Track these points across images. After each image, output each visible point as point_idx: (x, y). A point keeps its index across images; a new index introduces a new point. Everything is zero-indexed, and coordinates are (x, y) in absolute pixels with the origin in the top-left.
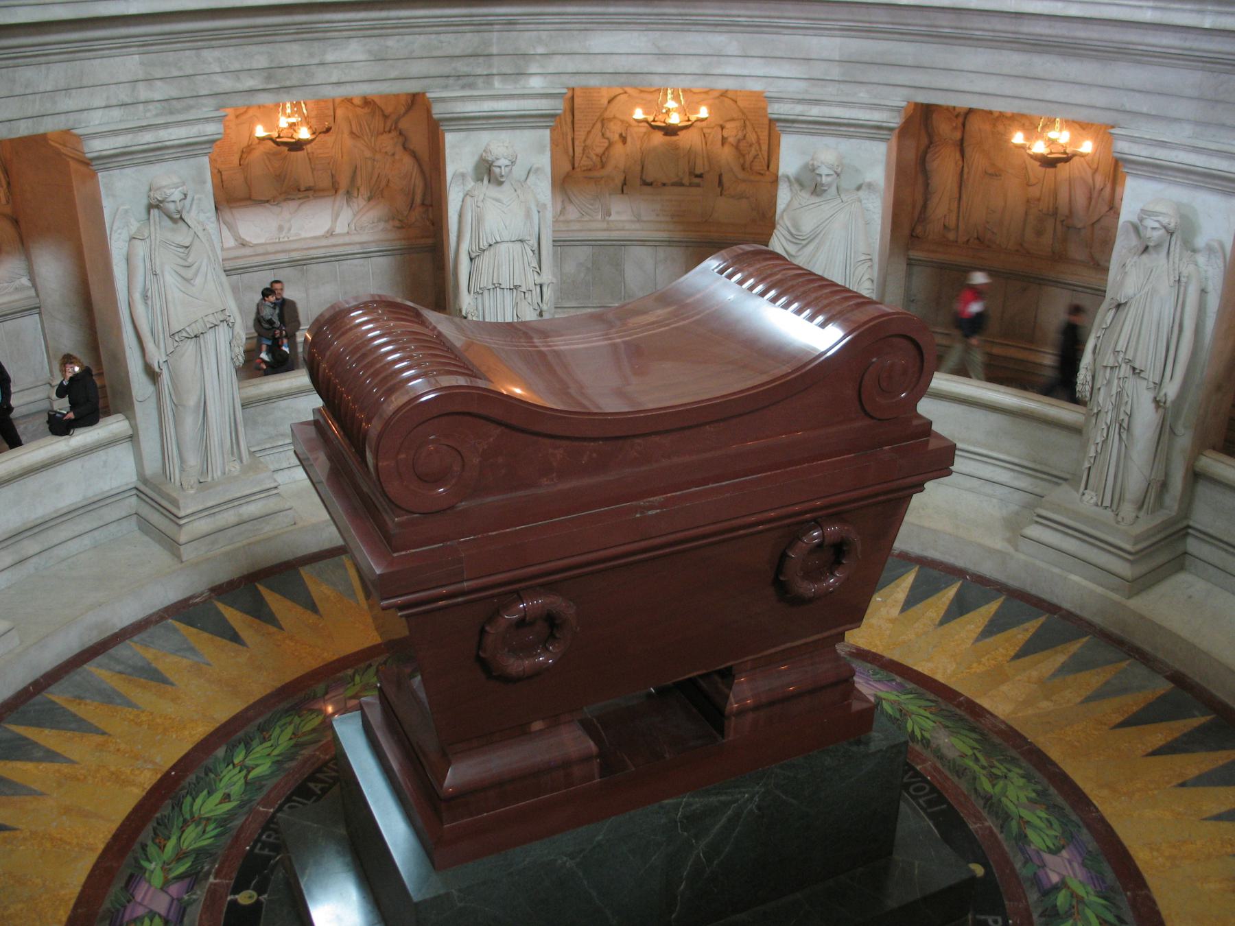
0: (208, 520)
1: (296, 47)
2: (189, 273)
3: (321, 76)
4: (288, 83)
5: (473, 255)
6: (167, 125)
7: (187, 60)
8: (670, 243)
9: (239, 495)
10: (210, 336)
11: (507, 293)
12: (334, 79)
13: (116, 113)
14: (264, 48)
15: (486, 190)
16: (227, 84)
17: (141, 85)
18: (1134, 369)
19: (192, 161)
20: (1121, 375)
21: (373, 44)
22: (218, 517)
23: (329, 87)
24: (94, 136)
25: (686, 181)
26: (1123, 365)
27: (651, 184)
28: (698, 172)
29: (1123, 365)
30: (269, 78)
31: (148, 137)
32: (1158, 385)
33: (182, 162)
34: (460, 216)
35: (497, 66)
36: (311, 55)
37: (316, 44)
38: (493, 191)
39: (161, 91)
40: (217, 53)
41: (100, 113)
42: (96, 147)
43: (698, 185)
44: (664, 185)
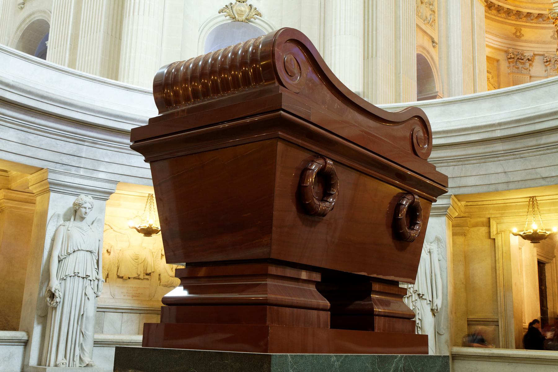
5: (62, 258)
8: (131, 311)
15: (72, 224)
18: (419, 294)
20: (414, 300)
25: (141, 277)
26: (413, 295)
27: (122, 278)
28: (148, 272)
29: (413, 295)
32: (432, 302)
34: (53, 240)
35: (83, 163)
38: (78, 223)
43: (148, 279)
44: (129, 278)
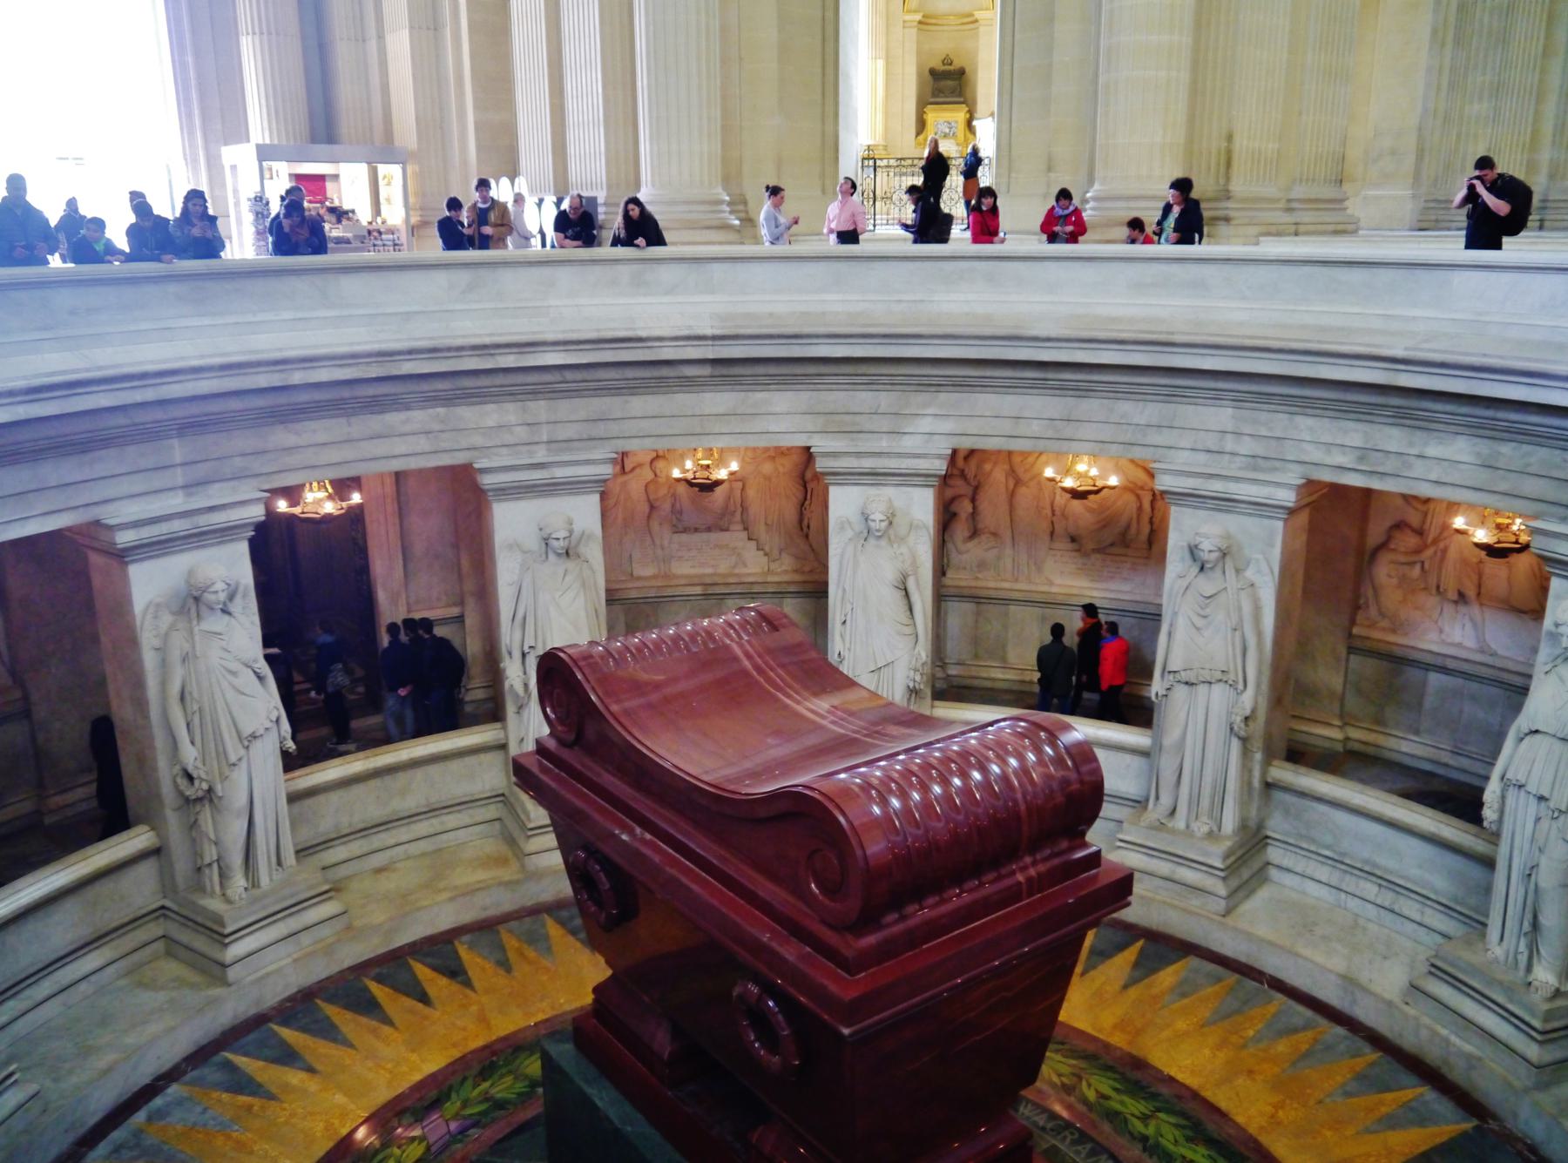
0: (1145, 858)
1: (1395, 432)
2: (1200, 622)
3: (1419, 469)
4: (1380, 469)
6: (1237, 479)
7: (1277, 422)
9: (1180, 853)
10: (1202, 689)
11: (1533, 802)
12: (1433, 477)
13: (1202, 457)
14: (1360, 426)
16: (1316, 455)
17: (1229, 436)
19: (1266, 522)
21: (1484, 447)
22: (1155, 861)
23: (1427, 485)
24: (1166, 472)
30: (1361, 459)
31: (1217, 486)
33: (1257, 520)
36: (1411, 444)
37: (1419, 433)
39: (1247, 447)
40: (1310, 421)
41: (1187, 453)
42: (1164, 482)
